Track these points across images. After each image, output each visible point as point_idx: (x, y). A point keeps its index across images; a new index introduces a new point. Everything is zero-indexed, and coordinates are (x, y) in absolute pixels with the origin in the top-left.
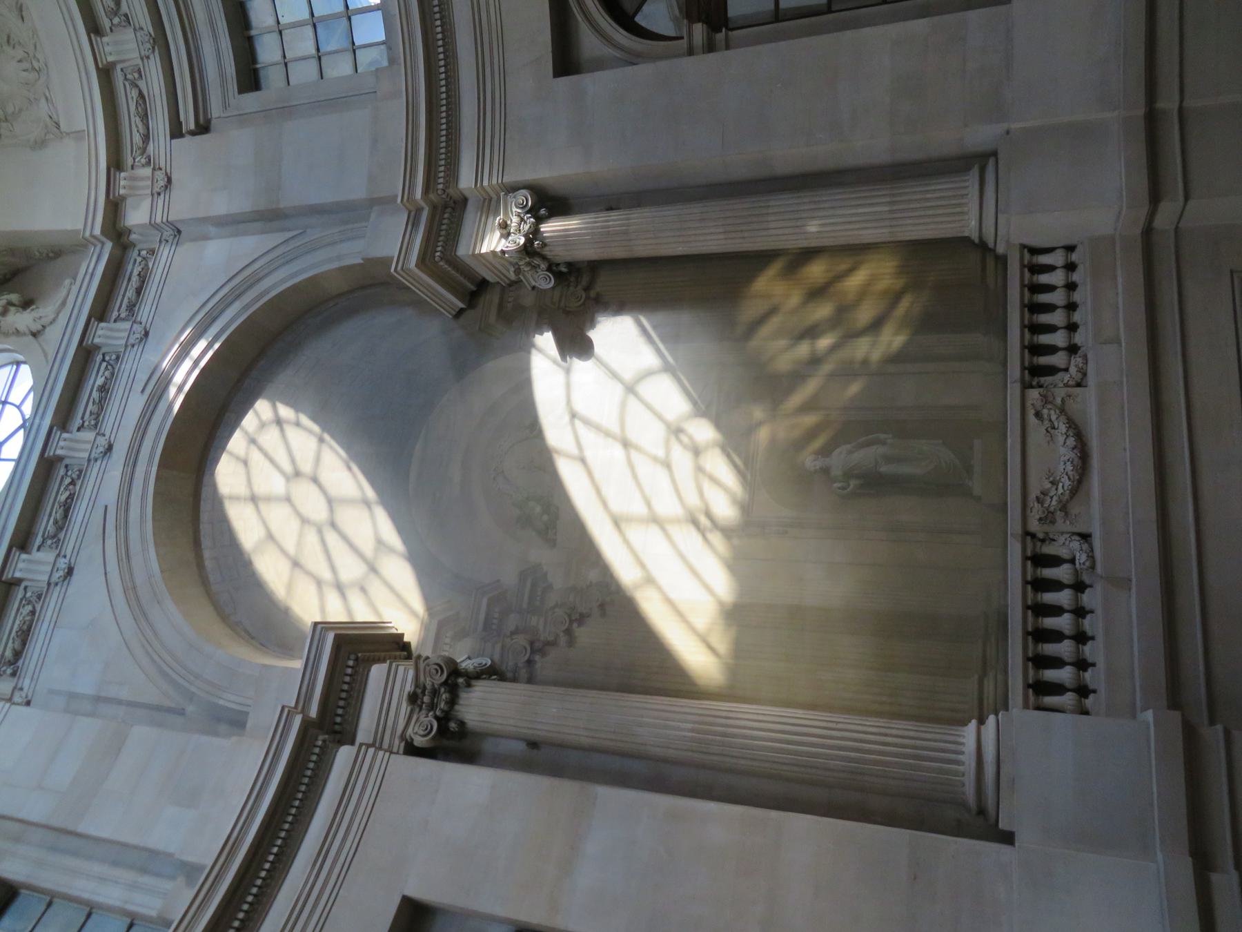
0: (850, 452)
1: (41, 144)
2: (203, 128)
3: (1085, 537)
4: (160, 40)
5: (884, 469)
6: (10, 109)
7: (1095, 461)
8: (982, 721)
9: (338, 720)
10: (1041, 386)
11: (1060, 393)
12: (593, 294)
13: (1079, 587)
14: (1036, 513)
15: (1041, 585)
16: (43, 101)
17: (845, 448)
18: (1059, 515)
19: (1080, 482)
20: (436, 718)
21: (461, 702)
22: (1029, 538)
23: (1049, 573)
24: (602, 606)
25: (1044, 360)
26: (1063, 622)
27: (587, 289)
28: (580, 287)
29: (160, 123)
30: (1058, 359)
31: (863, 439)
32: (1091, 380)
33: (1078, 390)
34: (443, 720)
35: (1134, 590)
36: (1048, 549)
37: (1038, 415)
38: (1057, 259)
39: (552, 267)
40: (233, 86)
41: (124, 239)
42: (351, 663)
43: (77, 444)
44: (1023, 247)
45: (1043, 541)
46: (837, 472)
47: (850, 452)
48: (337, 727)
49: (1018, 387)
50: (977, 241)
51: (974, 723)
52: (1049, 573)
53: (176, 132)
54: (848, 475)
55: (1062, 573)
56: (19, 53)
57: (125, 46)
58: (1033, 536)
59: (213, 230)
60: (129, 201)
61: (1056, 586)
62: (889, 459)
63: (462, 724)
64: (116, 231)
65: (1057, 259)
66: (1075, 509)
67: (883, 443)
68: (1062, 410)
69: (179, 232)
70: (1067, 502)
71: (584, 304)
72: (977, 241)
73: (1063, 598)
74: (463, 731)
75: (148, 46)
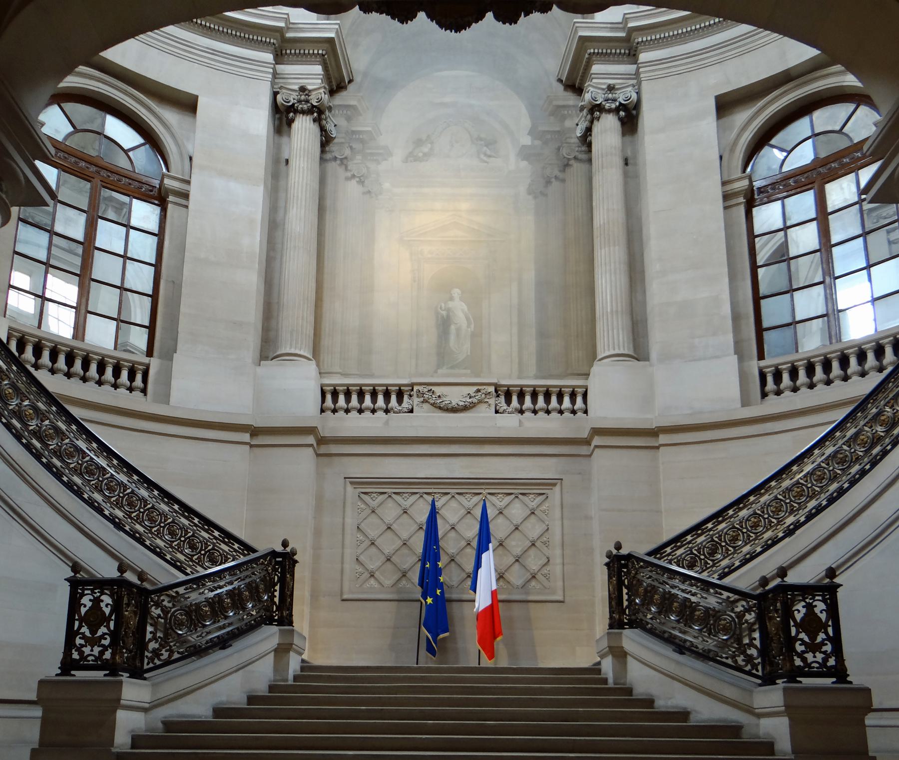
0: (463, 311)
3: (411, 411)
5: (453, 327)
9: (288, 52)
17: (465, 308)
18: (422, 399)
19: (440, 408)
20: (293, 104)
21: (304, 117)
24: (369, 192)
27: (575, 158)
34: (292, 109)
37: (478, 391)
39: (589, 130)
42: (320, 52)
46: (451, 304)
47: (463, 311)
48: (284, 52)
54: (448, 310)
62: (458, 330)
63: (293, 121)
66: (426, 406)
67: (469, 326)
74: (290, 122)
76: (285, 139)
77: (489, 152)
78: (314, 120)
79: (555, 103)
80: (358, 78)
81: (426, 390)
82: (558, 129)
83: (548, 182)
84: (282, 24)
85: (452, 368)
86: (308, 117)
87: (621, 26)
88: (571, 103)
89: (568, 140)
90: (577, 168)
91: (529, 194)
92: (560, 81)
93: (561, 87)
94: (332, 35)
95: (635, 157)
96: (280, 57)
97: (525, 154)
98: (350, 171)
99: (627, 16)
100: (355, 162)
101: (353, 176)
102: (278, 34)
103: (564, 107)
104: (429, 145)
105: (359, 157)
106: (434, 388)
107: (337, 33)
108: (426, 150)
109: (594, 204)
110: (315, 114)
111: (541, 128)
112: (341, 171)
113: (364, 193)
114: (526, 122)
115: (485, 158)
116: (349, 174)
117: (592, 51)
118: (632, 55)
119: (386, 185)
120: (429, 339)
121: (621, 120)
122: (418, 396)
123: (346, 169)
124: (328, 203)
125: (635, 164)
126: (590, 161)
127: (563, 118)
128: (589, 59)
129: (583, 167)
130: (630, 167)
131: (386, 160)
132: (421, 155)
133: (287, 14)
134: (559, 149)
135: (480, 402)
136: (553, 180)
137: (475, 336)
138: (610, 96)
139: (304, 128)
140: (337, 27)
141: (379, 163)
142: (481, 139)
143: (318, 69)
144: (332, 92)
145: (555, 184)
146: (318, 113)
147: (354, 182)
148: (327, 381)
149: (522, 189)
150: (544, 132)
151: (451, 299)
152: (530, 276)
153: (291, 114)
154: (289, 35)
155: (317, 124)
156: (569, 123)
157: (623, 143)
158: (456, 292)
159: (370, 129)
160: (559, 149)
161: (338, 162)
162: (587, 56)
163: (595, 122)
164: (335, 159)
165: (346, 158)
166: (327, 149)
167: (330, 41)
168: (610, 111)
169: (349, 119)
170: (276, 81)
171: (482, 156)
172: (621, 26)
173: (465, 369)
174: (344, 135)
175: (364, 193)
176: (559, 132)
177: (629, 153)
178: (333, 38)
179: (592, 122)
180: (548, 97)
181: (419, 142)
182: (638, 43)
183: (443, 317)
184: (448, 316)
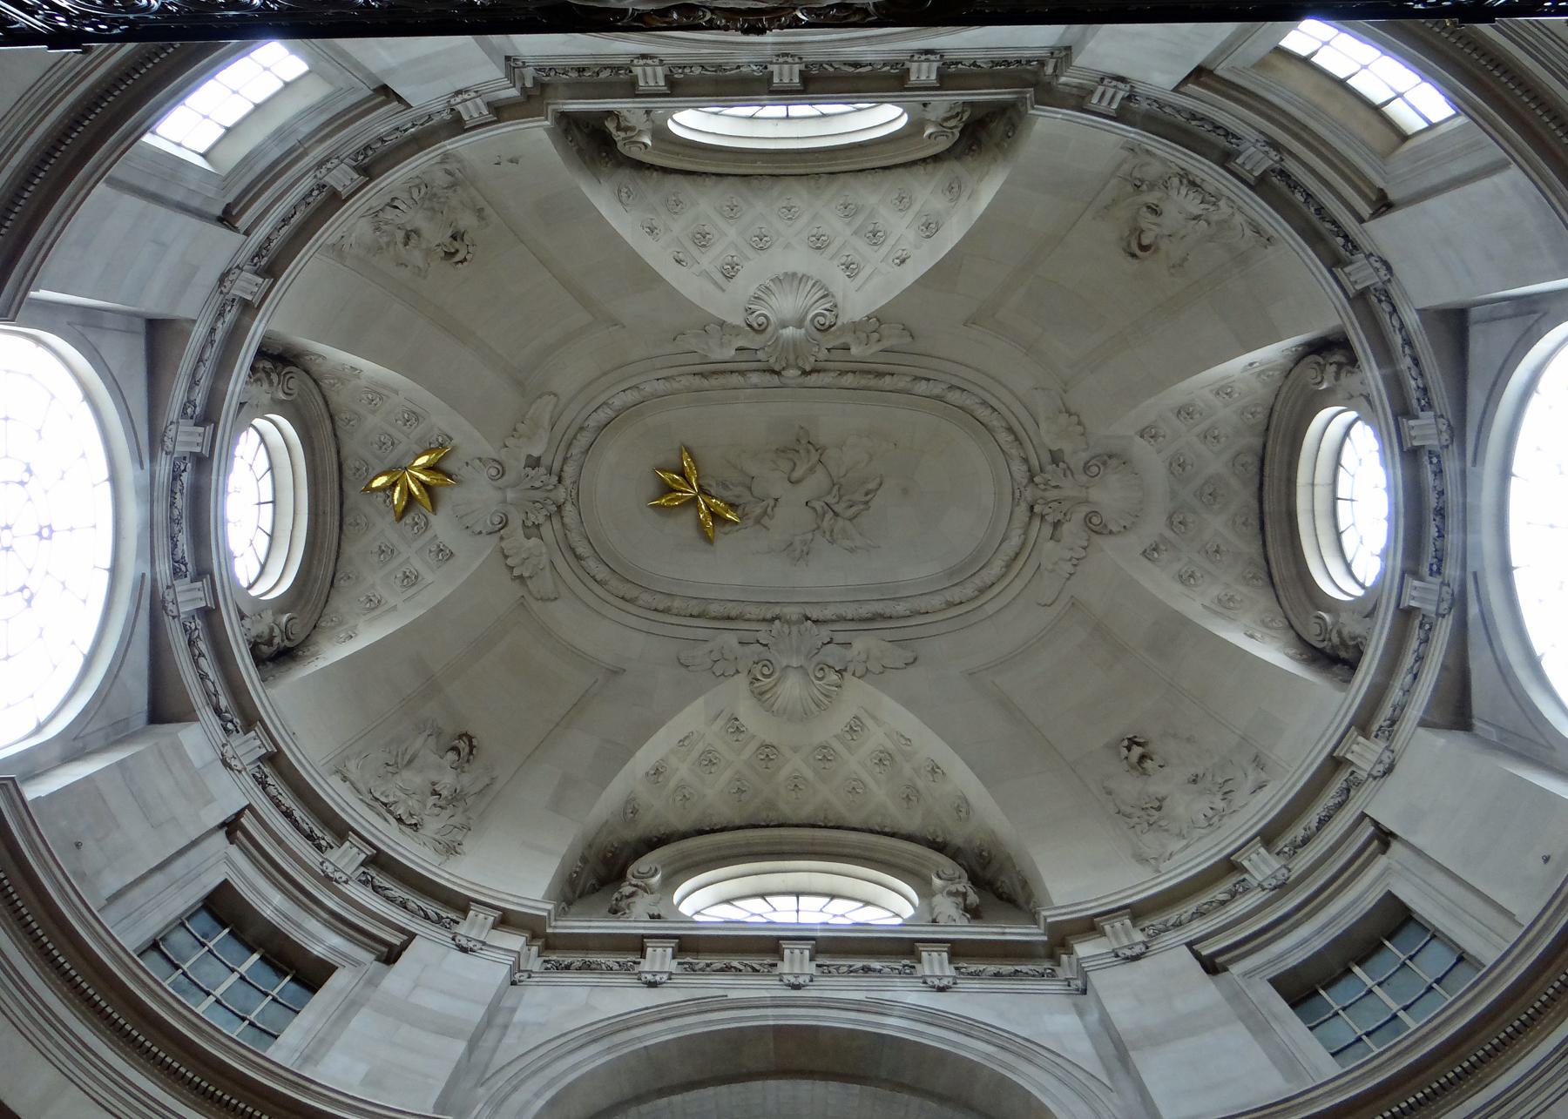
1: (1142, 859)
2: (1211, 966)
4: (1283, 888)
6: (1162, 823)
16: (1184, 842)
29: (1197, 929)
40: (1274, 972)
41: (1058, 951)
43: (796, 963)
53: (1190, 945)
56: (1220, 805)
57: (1263, 866)
59: (1093, 1017)
60: (1103, 939)
64: (1060, 940)
69: (1084, 992)
75: (1274, 882)
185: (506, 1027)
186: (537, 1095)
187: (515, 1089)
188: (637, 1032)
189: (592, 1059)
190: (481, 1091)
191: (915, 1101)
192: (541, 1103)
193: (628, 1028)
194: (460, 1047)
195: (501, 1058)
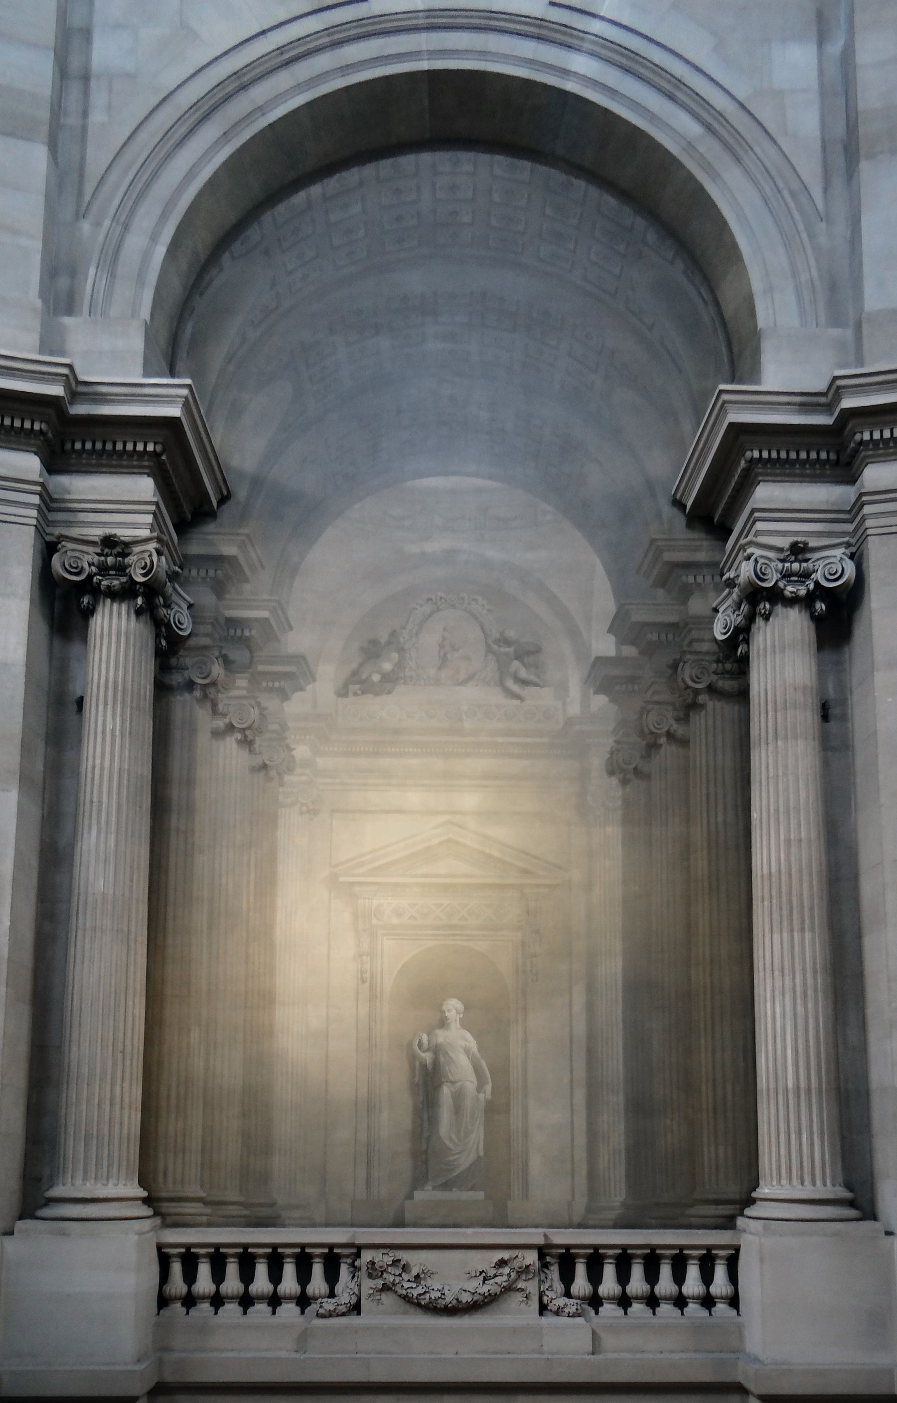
0: (467, 1051)
3: (356, 1308)
5: (446, 1091)
7: (445, 1322)
8: (147, 1201)
10: (545, 1265)
11: (532, 1287)
12: (702, 698)
13: (303, 1301)
14: (382, 1259)
15: (304, 1263)
17: (473, 1044)
18: (379, 1283)
19: (419, 1305)
20: (90, 577)
22: (354, 1251)
23: (318, 1270)
25: (581, 1270)
26: (261, 1283)
27: (711, 689)
28: (714, 678)
30: (581, 1284)
31: (484, 1064)
32: (548, 1320)
33: (535, 1306)
34: (88, 587)
35: (297, 1356)
36: (344, 1271)
38: (720, 1284)
39: (741, 634)
42: (150, 447)
44: (737, 1249)
45: (353, 1265)
46: (441, 1036)
47: (467, 1051)
48: (68, 446)
49: (541, 1241)
50: (754, 1195)
51: (145, 1194)
52: (318, 1270)
54: (436, 1050)
55: (317, 1284)
58: (358, 1255)
59: (835, 48)
61: (304, 1277)
62: (458, 1097)
63: (89, 612)
65: (720, 1284)
66: (387, 1299)
67: (480, 1089)
68: (509, 1289)
70: (396, 1292)
71: (688, 687)
72: (754, 1195)
73: (289, 1284)
76: (76, 648)
77: (523, 674)
78: (139, 612)
79: (668, 556)
80: (241, 492)
81: (388, 1260)
82: (673, 618)
83: (652, 747)
84: (57, 390)
85: (447, 1186)
86: (124, 607)
87: (822, 400)
88: (702, 556)
89: (696, 647)
90: (716, 711)
91: (611, 773)
92: (678, 504)
93: (680, 521)
94: (174, 411)
95: (843, 702)
96: (56, 461)
97: (605, 677)
98: (224, 715)
99: (840, 383)
100: (235, 693)
101: (231, 728)
102: (51, 411)
103: (688, 566)
104: (395, 656)
105: (242, 682)
106: (405, 1256)
107: (186, 406)
108: (387, 666)
109: (755, 815)
110: (140, 601)
111: (640, 616)
112: (202, 714)
113: (254, 770)
114: (605, 603)
115: (515, 688)
116: (221, 723)
117: (756, 454)
118: (845, 469)
119: (301, 751)
120: (395, 1119)
121: (818, 620)
122: (370, 1276)
123: (215, 712)
124: (175, 793)
125: (844, 718)
126: (743, 695)
127: (685, 593)
128: (747, 472)
129: (727, 710)
130: (833, 725)
131: (301, 689)
132: (376, 678)
133: (70, 366)
134: (675, 667)
135: (509, 1289)
136: (663, 740)
137: (495, 1110)
138: (796, 566)
139: (115, 637)
140: (185, 392)
141: (285, 696)
142: (507, 642)
143: (143, 487)
144: (183, 527)
145: (668, 750)
146: (148, 598)
147: (231, 743)
148: (173, 1236)
149: (597, 762)
150: (645, 624)
151: (443, 1023)
152: (612, 969)
153: (86, 600)
154: (80, 409)
155: (146, 618)
156: (697, 606)
157: (821, 674)
158: (453, 1007)
159: (265, 614)
160: (675, 667)
161: (198, 693)
162: (743, 463)
163: (759, 621)
164: (190, 685)
165: (214, 684)
166: (173, 661)
167: (172, 423)
168: (793, 601)
169: (219, 588)
170: (51, 516)
171: (510, 684)
172: (822, 400)
173: (473, 1188)
174: (209, 629)
175: (254, 770)
176: (674, 626)
177: (831, 693)
178: (177, 419)
179: (750, 619)
180: (653, 541)
181: (372, 651)
182: (861, 443)
183: (424, 1066)
184: (436, 1063)
185: (86, 78)
186: (154, 238)
187: (126, 227)
188: (259, 93)
189: (204, 156)
190: (86, 226)
191: (594, 192)
192: (161, 250)
193: (244, 87)
194: (40, 154)
195: (97, 159)
